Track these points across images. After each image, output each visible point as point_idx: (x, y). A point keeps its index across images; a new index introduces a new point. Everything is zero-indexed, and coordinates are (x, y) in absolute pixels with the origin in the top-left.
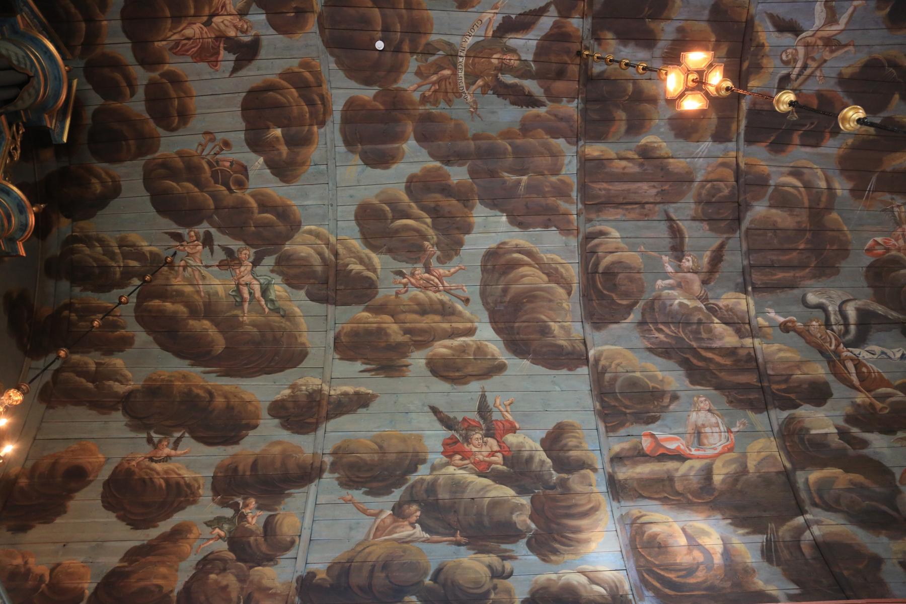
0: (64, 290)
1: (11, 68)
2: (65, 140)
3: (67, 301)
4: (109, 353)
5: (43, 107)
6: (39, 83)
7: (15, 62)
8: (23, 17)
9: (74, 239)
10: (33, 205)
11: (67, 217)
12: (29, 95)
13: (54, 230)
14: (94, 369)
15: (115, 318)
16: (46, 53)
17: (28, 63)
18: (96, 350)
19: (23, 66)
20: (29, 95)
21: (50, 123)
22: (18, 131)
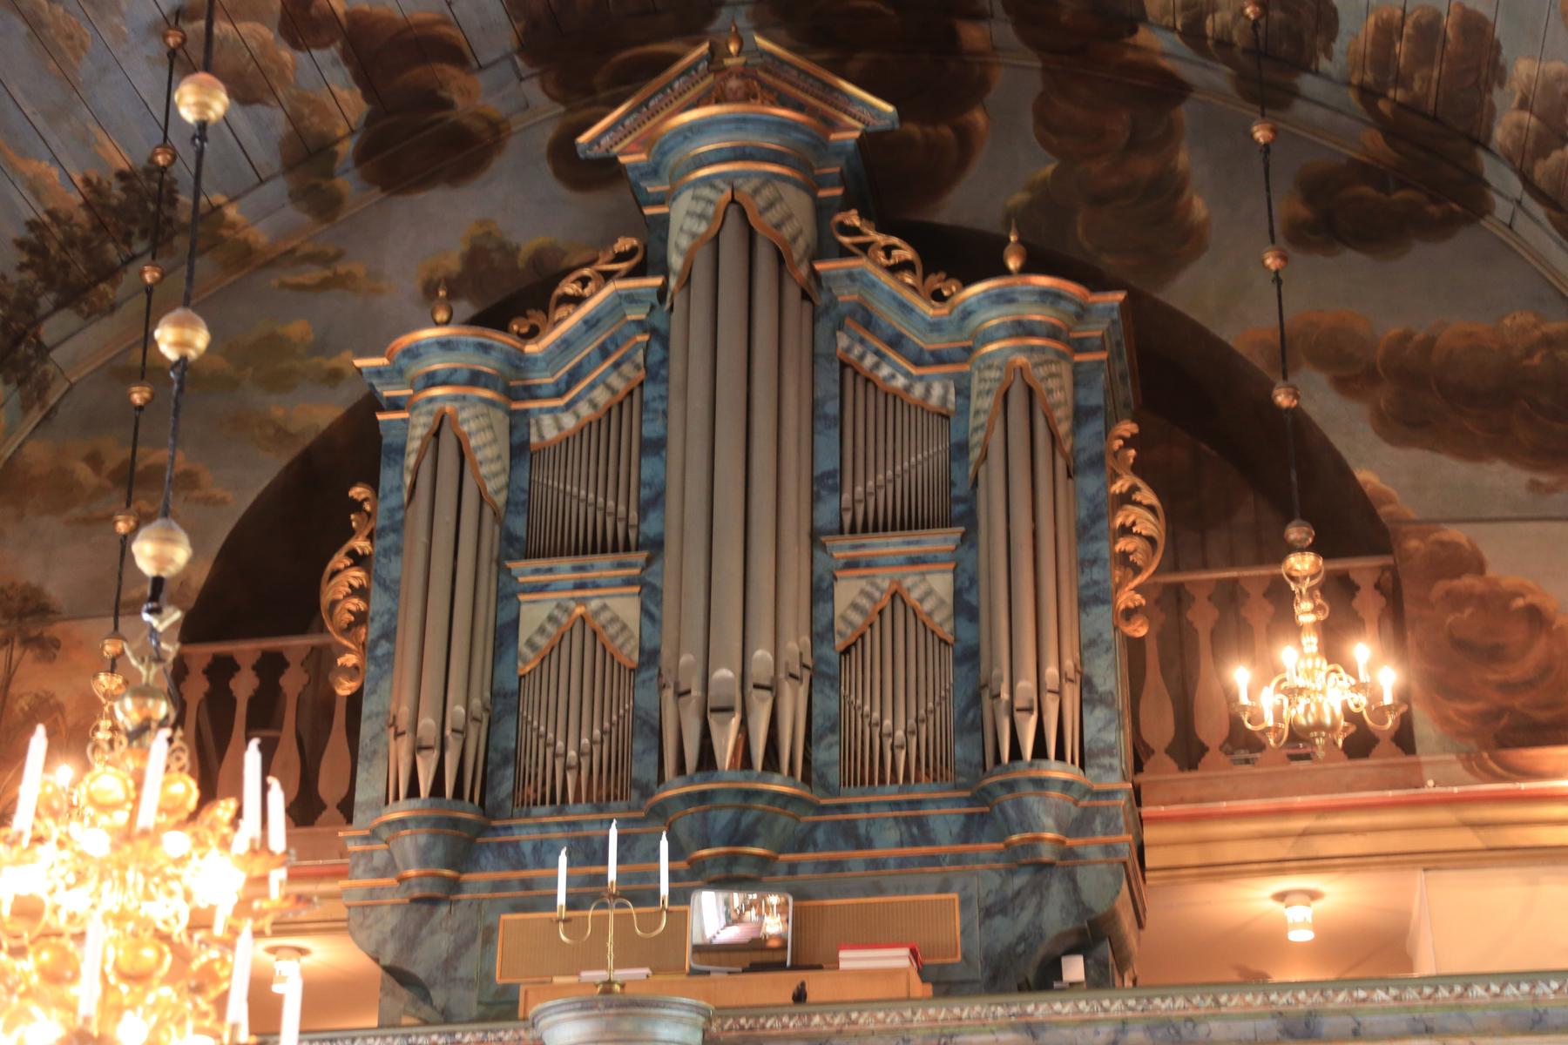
0: (1327, 84)
1: (716, 238)
2: (889, 108)
3: (1352, 96)
4: (1498, 73)
5: (804, 160)
6: (747, 175)
7: (702, 228)
8: (623, 153)
9: (1193, 33)
10: (1002, 271)
11: (1134, 31)
12: (770, 205)
13: (1167, 64)
14: (1533, 120)
15: (1409, 22)
16: (686, 138)
17: (706, 192)
18: (1490, 91)
19: (711, 210)
20: (770, 205)
21: (848, 136)
22: (855, 231)
